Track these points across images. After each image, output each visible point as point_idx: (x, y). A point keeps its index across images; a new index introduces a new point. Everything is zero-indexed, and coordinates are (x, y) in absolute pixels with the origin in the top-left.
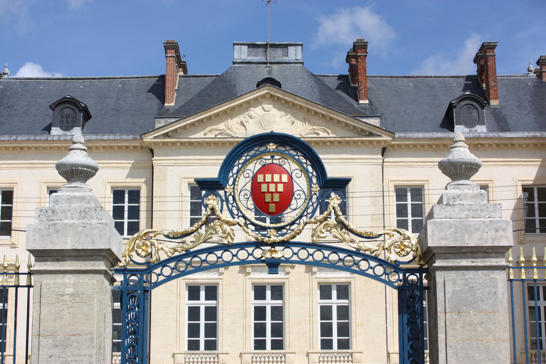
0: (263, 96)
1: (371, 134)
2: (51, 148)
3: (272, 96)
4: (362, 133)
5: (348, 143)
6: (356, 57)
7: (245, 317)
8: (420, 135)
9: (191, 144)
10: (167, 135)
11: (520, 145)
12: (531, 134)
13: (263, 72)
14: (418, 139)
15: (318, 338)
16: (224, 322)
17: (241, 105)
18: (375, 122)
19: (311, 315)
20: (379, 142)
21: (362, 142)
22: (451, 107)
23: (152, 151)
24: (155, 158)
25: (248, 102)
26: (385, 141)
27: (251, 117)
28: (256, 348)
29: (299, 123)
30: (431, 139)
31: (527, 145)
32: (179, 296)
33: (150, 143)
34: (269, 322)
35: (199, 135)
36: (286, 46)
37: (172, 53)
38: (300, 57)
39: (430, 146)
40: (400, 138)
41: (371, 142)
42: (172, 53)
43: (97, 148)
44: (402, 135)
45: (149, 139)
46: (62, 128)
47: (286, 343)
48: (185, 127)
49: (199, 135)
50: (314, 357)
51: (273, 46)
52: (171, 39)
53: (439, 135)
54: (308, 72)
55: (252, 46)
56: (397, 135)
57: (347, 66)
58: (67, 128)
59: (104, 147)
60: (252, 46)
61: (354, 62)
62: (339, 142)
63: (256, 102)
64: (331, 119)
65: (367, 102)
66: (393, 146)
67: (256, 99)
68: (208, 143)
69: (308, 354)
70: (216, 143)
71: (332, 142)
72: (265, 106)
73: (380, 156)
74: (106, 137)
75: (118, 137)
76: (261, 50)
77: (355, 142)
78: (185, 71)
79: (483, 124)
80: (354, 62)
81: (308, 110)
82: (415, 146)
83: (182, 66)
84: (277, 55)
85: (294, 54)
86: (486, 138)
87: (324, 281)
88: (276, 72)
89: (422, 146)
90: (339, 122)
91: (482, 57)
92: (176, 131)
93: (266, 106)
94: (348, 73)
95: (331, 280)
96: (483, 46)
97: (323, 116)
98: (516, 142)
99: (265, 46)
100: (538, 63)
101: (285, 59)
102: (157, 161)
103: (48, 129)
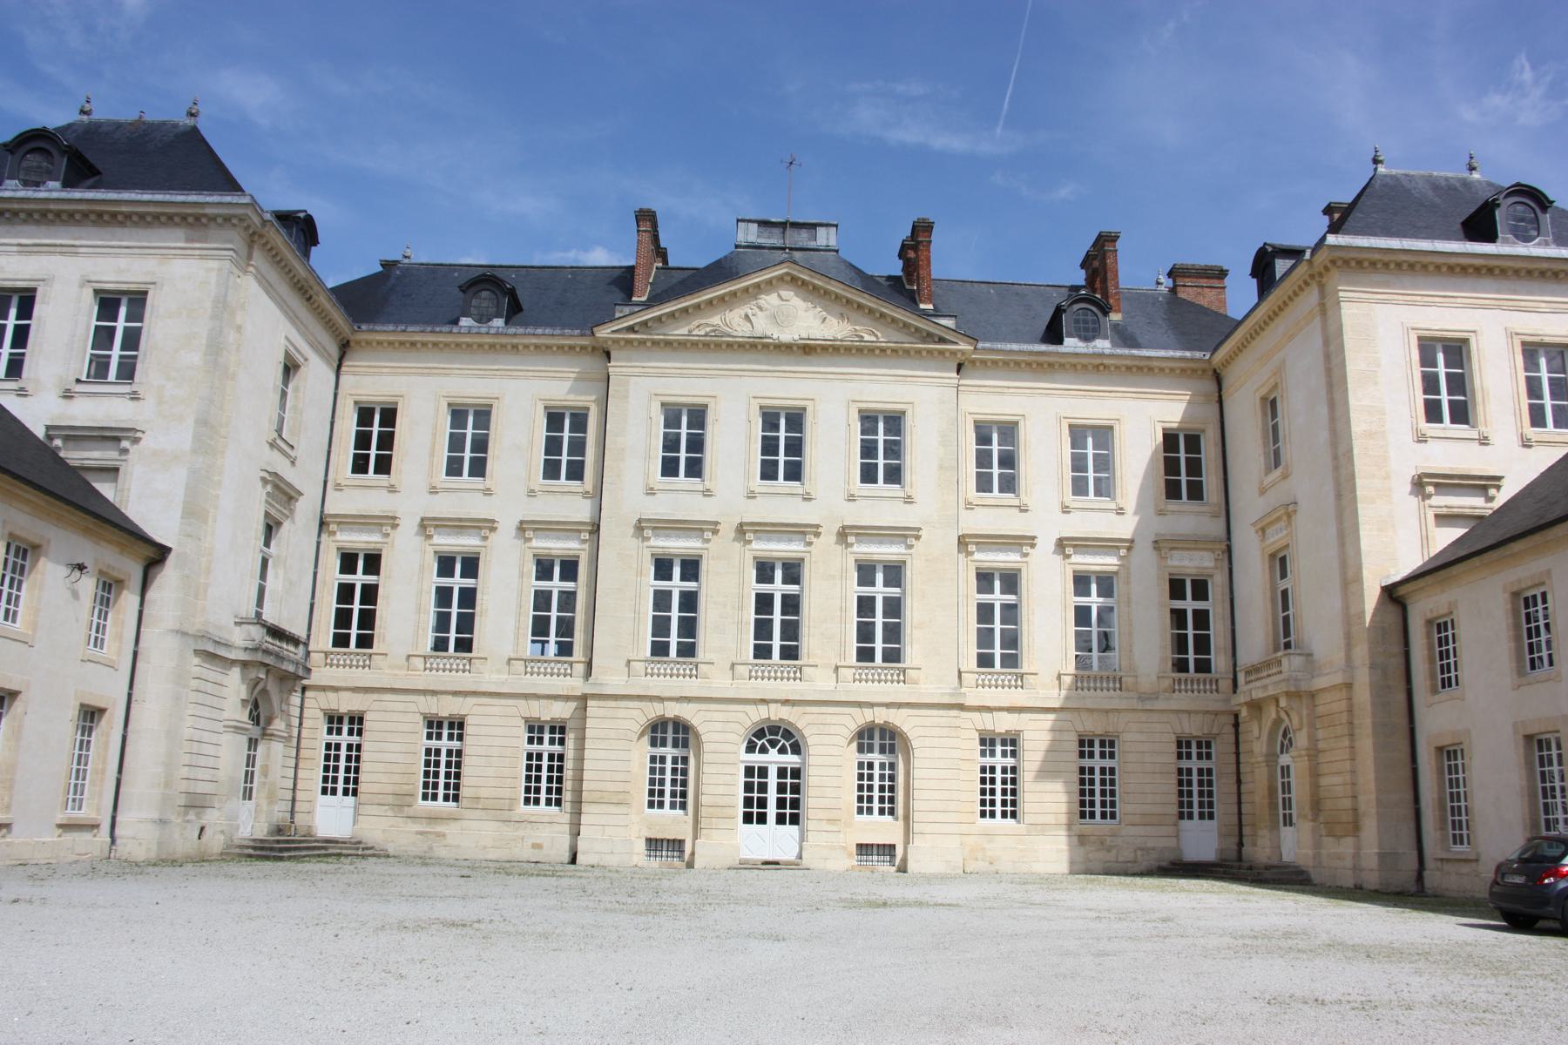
0: (781, 278)
1: (942, 340)
2: (458, 345)
3: (794, 279)
4: (929, 337)
5: (907, 352)
6: (915, 248)
7: (741, 608)
8: (1015, 347)
9: (668, 344)
10: (631, 329)
11: (1162, 370)
12: (1178, 354)
14: (1011, 351)
15: (853, 645)
16: (707, 615)
17: (746, 290)
19: (843, 610)
20: (953, 353)
21: (929, 352)
22: (1059, 312)
23: (608, 355)
25: (757, 286)
26: (963, 352)
27: (761, 308)
28: (756, 657)
29: (833, 321)
30: (1031, 353)
31: (1172, 370)
32: (640, 573)
34: (777, 617)
35: (680, 331)
36: (814, 226)
37: (646, 226)
38: (833, 243)
39: (1029, 364)
41: (941, 352)
43: (526, 347)
44: (988, 345)
45: (604, 332)
47: (804, 651)
48: (659, 319)
49: (680, 331)
50: (847, 673)
51: (796, 225)
52: (645, 207)
53: (1043, 347)
54: (845, 261)
55: (764, 224)
56: (980, 345)
57: (900, 263)
58: (483, 319)
59: (537, 347)
60: (764, 224)
61: (911, 254)
62: (894, 351)
63: (770, 285)
64: (882, 315)
65: (931, 307)
66: (973, 362)
67: (769, 282)
68: (695, 344)
69: (837, 668)
70: (706, 345)
71: (883, 350)
72: (783, 293)
76: (777, 231)
77: (919, 352)
78: (665, 261)
79: (1105, 338)
80: (911, 254)
81: (848, 301)
82: (1006, 363)
83: (662, 254)
84: (802, 238)
85: (824, 238)
86: (1111, 356)
87: (864, 557)
89: (1017, 364)
90: (894, 320)
91: (1095, 257)
92: (645, 324)
93: (785, 293)
94: (899, 273)
95: (876, 557)
96: (1100, 236)
97: (871, 311)
98: (1155, 364)
99: (783, 225)
100: (1170, 275)
101: (812, 244)
102: (616, 368)
103: (456, 322)
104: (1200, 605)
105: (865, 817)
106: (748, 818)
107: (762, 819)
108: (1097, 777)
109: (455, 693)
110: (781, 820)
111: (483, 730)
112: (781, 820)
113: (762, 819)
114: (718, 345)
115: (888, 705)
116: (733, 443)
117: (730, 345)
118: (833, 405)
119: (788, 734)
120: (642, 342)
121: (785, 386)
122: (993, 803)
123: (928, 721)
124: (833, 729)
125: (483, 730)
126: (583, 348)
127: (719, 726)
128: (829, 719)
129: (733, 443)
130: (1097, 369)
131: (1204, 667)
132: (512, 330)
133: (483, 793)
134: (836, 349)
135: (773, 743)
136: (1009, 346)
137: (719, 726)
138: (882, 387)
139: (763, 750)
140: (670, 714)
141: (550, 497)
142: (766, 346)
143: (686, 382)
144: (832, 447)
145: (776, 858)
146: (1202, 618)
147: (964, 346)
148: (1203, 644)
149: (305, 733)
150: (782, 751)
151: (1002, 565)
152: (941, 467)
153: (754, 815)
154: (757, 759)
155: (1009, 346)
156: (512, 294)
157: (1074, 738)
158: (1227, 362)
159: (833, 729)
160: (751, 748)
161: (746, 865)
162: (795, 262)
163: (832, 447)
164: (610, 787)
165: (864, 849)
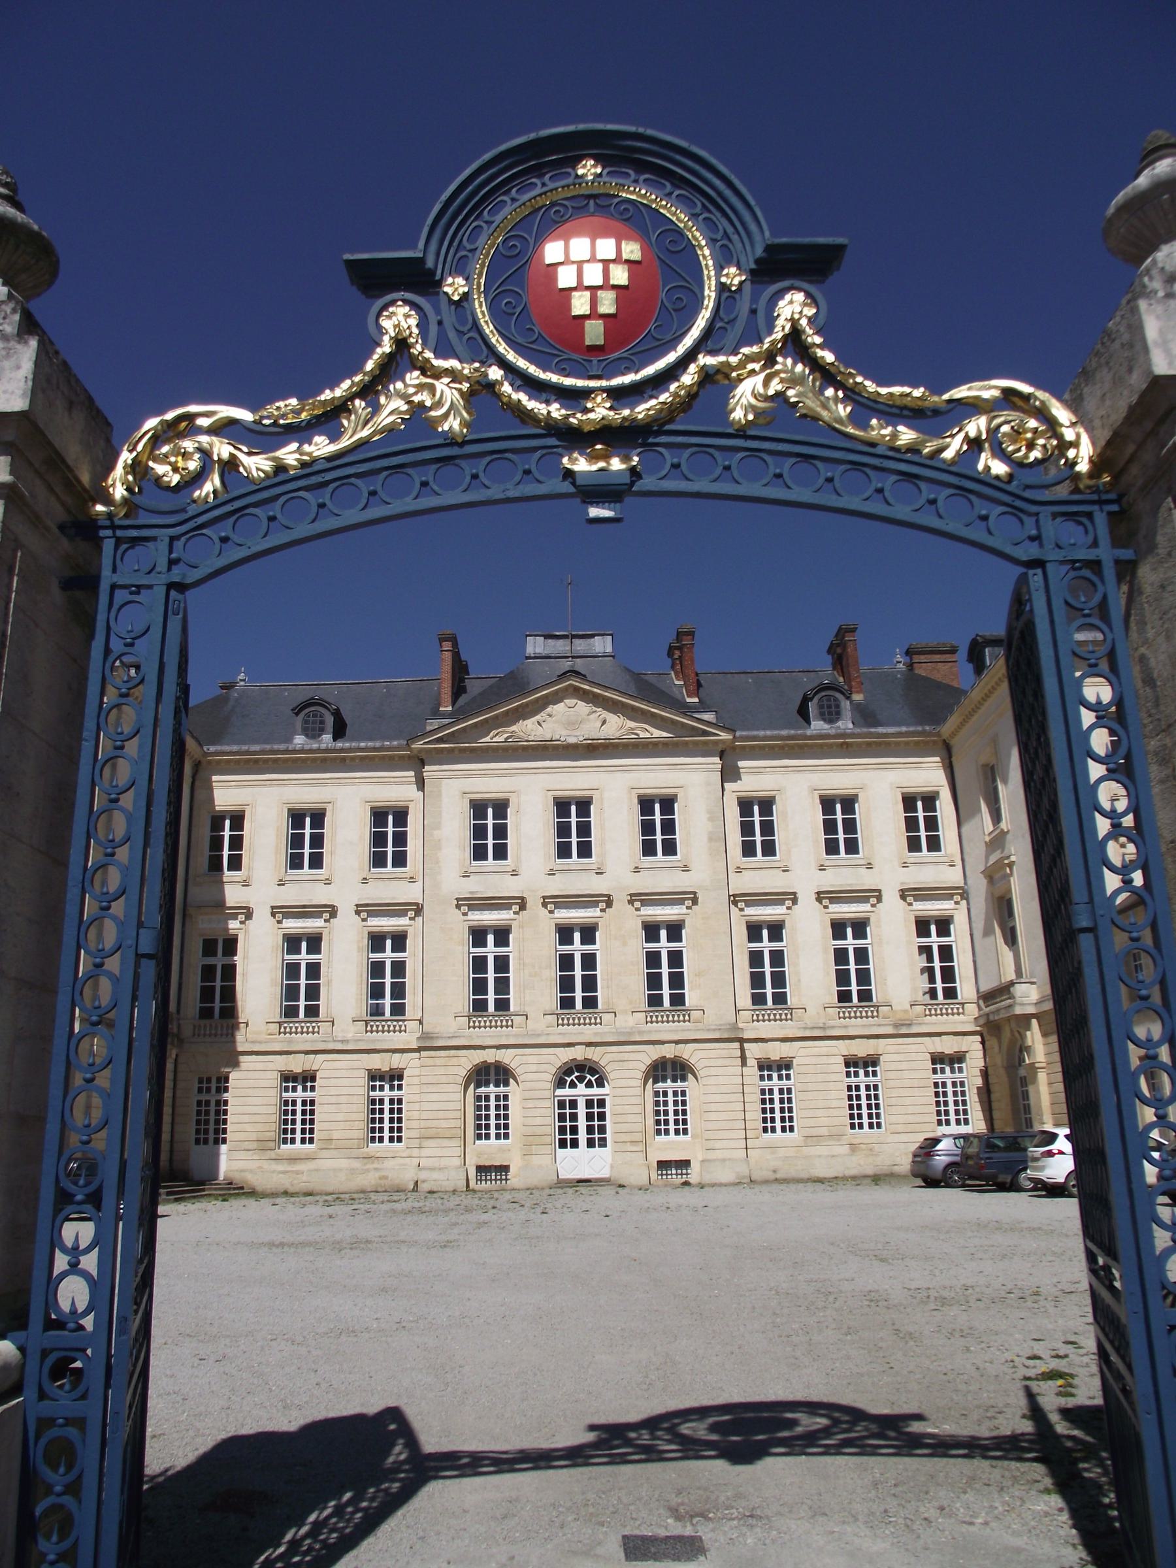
0: (566, 689)
5: (676, 744)
10: (440, 740)
13: (567, 664)
18: (709, 717)
20: (716, 743)
21: (696, 743)
24: (427, 768)
27: (550, 716)
33: (421, 750)
40: (743, 739)
41: (706, 743)
42: (447, 646)
46: (307, 736)
56: (738, 734)
70: (505, 749)
73: (717, 760)
74: (363, 744)
75: (378, 744)
86: (852, 735)
87: (649, 919)
88: (579, 665)
93: (570, 702)
104: (944, 940)
105: (663, 1138)
106: (563, 1144)
107: (575, 1144)
108: (863, 1093)
109: (307, 1053)
110: (590, 1144)
111: (333, 1082)
112: (590, 1144)
113: (575, 1144)
114: (515, 749)
115: (677, 1042)
116: (530, 828)
117: (525, 748)
118: (614, 791)
119: (593, 1071)
120: (452, 750)
121: (574, 778)
122: (773, 1120)
123: (713, 1054)
124: (631, 1065)
125: (333, 1082)
126: (401, 757)
127: (534, 1068)
128: (626, 1056)
129: (530, 828)
130: (844, 748)
131: (950, 993)
132: (339, 745)
133: (336, 1135)
134: (615, 746)
135: (581, 1079)
136: (761, 733)
137: (534, 1068)
138: (656, 775)
139: (573, 1085)
140: (491, 1060)
141: (380, 883)
142: (556, 747)
143: (489, 780)
144: (616, 827)
145: (586, 1176)
146: (946, 953)
147: (724, 736)
148: (948, 974)
149: (179, 1093)
150: (589, 1085)
151: (768, 918)
152: (710, 839)
153: (567, 1141)
154: (566, 1092)
155: (761, 733)
156: (337, 714)
157: (841, 1060)
158: (953, 734)
159: (631, 1065)
160: (560, 1083)
161: (563, 1184)
162: (576, 673)
163: (616, 827)
164: (444, 1124)
165: (663, 1165)
